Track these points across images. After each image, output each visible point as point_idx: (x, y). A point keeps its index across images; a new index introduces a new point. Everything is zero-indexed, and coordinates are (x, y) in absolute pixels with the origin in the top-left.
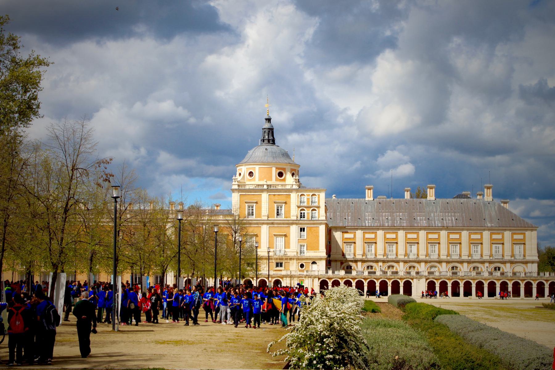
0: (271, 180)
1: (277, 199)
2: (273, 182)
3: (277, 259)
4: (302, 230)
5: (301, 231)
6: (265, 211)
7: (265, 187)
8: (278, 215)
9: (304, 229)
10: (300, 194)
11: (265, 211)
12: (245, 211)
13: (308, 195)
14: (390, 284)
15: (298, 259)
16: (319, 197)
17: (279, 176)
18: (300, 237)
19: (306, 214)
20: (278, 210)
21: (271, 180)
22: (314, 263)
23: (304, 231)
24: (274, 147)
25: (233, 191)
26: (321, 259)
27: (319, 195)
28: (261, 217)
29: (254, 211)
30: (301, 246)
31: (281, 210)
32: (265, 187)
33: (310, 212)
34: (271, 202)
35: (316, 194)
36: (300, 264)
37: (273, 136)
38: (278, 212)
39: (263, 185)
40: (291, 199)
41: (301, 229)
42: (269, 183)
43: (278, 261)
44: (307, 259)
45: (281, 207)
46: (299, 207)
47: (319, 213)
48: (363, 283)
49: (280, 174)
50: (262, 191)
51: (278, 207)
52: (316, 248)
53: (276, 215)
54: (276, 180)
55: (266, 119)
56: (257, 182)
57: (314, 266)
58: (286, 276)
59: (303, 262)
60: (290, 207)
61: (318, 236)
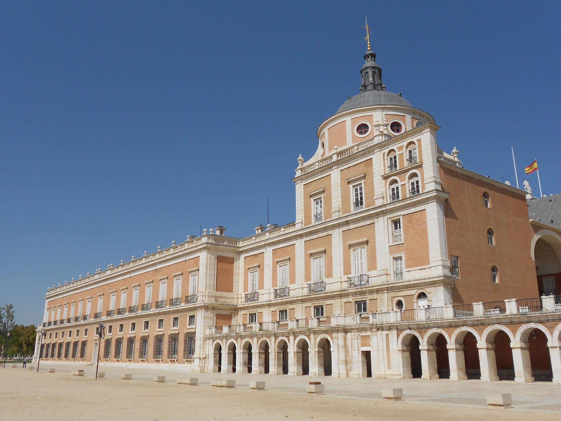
1: (352, 174)
3: (355, 294)
4: (396, 223)
7: (335, 158)
10: (387, 151)
11: (336, 202)
13: (400, 148)
15: (390, 289)
16: (420, 146)
22: (422, 295)
26: (433, 284)
30: (396, 259)
35: (414, 140)
36: (396, 300)
40: (374, 167)
43: (359, 298)
44: (407, 287)
46: (385, 178)
48: (509, 341)
57: (423, 303)
58: (337, 330)
60: (372, 183)
61: (425, 232)
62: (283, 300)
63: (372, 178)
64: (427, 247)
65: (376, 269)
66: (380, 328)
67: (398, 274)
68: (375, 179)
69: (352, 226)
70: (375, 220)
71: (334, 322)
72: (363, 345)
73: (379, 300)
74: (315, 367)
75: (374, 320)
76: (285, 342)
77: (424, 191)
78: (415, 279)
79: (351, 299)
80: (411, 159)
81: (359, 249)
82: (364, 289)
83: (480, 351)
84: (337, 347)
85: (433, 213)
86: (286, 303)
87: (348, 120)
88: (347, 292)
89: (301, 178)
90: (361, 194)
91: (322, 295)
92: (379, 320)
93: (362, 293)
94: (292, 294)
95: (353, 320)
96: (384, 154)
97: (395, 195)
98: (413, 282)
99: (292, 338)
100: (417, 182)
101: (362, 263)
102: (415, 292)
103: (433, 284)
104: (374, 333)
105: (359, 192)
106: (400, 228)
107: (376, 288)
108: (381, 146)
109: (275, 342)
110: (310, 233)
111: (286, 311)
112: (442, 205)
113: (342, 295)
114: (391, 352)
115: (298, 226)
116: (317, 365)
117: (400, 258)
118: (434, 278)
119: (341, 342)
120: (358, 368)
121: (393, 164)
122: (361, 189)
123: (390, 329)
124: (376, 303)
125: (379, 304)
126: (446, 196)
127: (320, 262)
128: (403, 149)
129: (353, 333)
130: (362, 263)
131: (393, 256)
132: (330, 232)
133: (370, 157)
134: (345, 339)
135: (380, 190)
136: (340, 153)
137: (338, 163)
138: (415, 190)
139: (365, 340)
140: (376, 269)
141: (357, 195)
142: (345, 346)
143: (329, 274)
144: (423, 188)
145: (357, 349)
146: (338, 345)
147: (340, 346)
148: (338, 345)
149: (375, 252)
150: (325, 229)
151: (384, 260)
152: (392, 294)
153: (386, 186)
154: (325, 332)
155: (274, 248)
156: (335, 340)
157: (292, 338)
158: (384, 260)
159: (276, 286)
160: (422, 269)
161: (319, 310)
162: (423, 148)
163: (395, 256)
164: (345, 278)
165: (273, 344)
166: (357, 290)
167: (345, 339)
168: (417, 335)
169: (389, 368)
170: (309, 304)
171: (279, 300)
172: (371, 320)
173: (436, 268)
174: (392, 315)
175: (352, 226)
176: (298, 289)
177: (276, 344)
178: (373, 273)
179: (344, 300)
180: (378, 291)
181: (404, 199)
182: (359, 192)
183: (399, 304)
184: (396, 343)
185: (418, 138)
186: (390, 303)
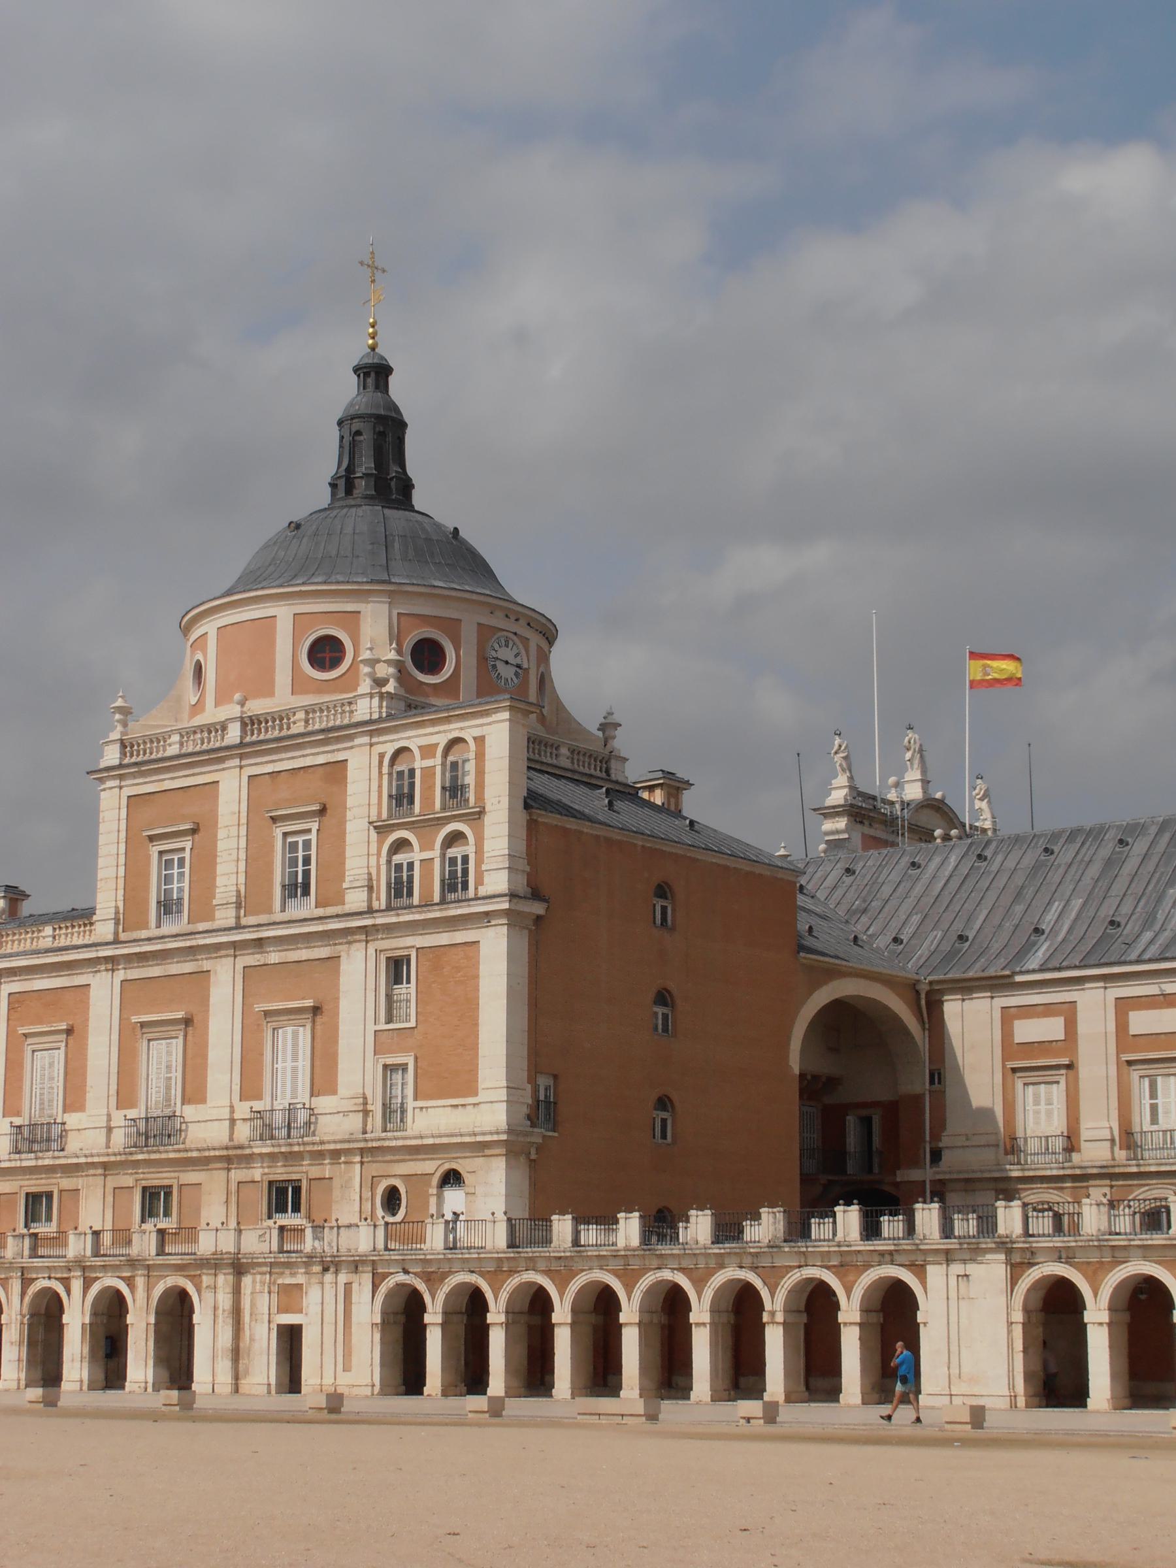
0: (271, 693)
2: (282, 697)
4: (397, 968)
6: (229, 877)
7: (234, 734)
10: (390, 749)
11: (229, 877)
12: (147, 889)
14: (775, 1304)
16: (480, 756)
17: (335, 662)
18: (389, 1020)
21: (271, 693)
22: (452, 1178)
25: (102, 774)
26: (480, 1148)
27: (480, 740)
32: (234, 734)
33: (436, 853)
34: (263, 815)
35: (468, 735)
40: (351, 789)
42: (257, 707)
43: (280, 1173)
46: (382, 830)
47: (479, 851)
49: (326, 652)
50: (216, 756)
52: (457, 1082)
54: (299, 684)
56: (212, 714)
58: (213, 1263)
59: (398, 1172)
62: (40, 1163)
63: (342, 823)
64: (475, 1047)
65: (333, 1091)
66: (330, 1265)
67: (393, 1113)
68: (350, 827)
69: (274, 957)
70: (342, 949)
71: (206, 1245)
72: (280, 1311)
73: (336, 1183)
74: (140, 1364)
75: (317, 1243)
76: (57, 1295)
77: (482, 891)
78: (435, 1132)
79: (257, 1173)
80: (454, 790)
81: (290, 1029)
82: (296, 1149)
83: (557, 1331)
84: (211, 1312)
85: (494, 953)
86: (51, 1170)
87: (283, 614)
88: (248, 1151)
89: (119, 771)
90: (307, 861)
91: (172, 1155)
92: (329, 1243)
93: (291, 1157)
94: (74, 1144)
95: (259, 1241)
96: (382, 756)
98: (430, 1141)
99: (77, 1285)
100: (465, 859)
101: (295, 1070)
102: (433, 1167)
103: (480, 1148)
104: (314, 1280)
105: (300, 854)
106: (408, 982)
107: (332, 1147)
108: (373, 728)
109: (23, 1294)
110: (143, 957)
111: (49, 1195)
112: (526, 932)
113: (232, 1157)
114: (353, 1330)
115: (104, 930)
116: (151, 1362)
117: (404, 1068)
118: (484, 1134)
119: (224, 1300)
120: (263, 1368)
121: (402, 798)
122: (307, 844)
123: (356, 1266)
124: (330, 1189)
125: (336, 1193)
126: (538, 909)
127: (169, 1053)
128: (434, 756)
129: (258, 1277)
130: (295, 1070)
131: (382, 1061)
132: (206, 965)
133: (340, 757)
134: (237, 1291)
135: (362, 856)
136: (249, 723)
137: (242, 750)
138: (455, 882)
139: (290, 1297)
140: (333, 1091)
141: (293, 862)
142: (236, 1312)
143: (194, 1092)
144: (479, 882)
145: (266, 1318)
146: (215, 1308)
147: (220, 1311)
148: (215, 1308)
149: (337, 1042)
150: (192, 951)
151: (357, 1070)
152: (374, 1169)
153: (379, 854)
154: (179, 1268)
155: (16, 986)
156: (208, 1296)
157: (77, 1285)
158: (357, 1070)
159: (18, 1114)
160: (457, 1106)
161: (154, 1200)
163: (389, 1061)
164: (243, 1109)
165: (16, 1299)
166: (276, 1150)
167: (237, 1291)
168: (421, 1286)
169: (347, 1368)
170: (126, 1180)
171: (28, 1161)
172: (309, 1243)
173: (490, 1109)
174: (365, 1232)
175: (274, 957)
176: (91, 1130)
177: (27, 1299)
178: (324, 1103)
179: (237, 1175)
180: (336, 1154)
181: (426, 905)
182: (300, 854)
183: (392, 1199)
184: (368, 1310)
185: (477, 732)
186: (367, 1194)
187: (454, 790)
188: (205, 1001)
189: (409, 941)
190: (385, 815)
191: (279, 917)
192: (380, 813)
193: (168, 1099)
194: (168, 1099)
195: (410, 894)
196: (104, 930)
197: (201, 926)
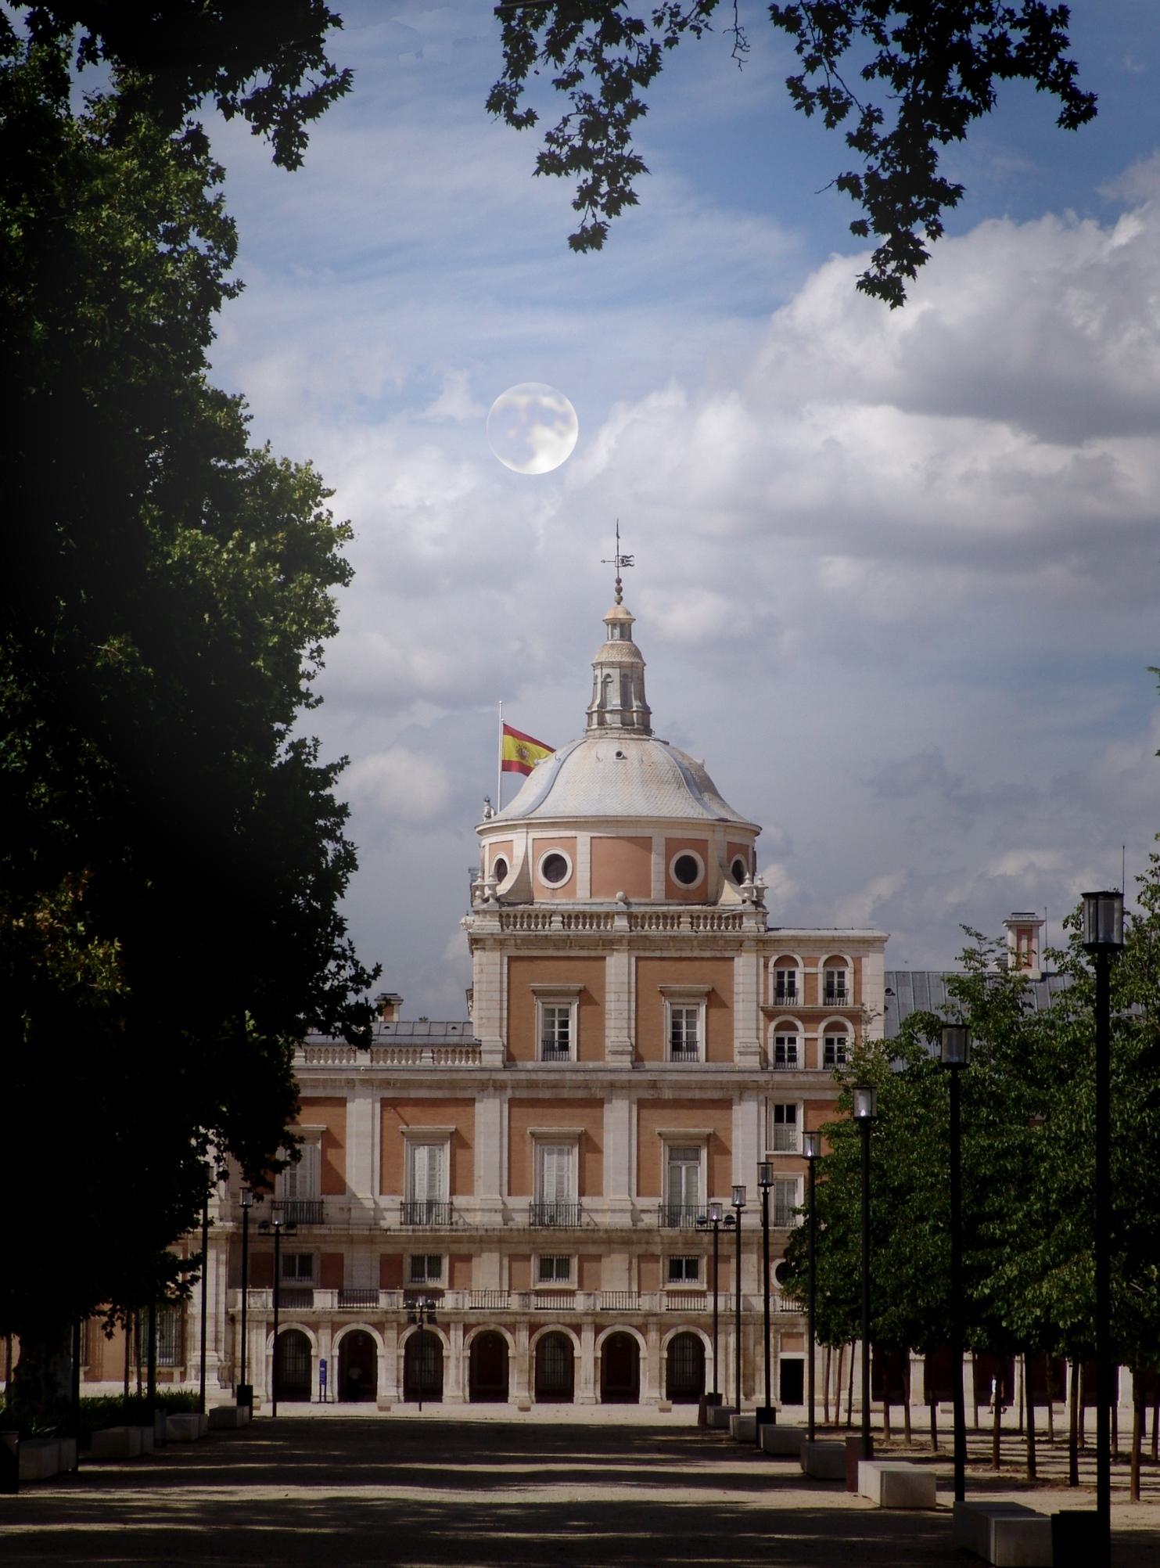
5: (779, 1119)
6: (617, 1030)
8: (676, 1047)
9: (792, 1110)
11: (617, 1030)
19: (800, 1045)
20: (676, 1026)
23: (792, 1119)
24: (651, 746)
28: (600, 1056)
29: (572, 1030)
31: (691, 1025)
37: (641, 697)
38: (676, 1036)
39: (609, 916)
41: (779, 1110)
45: (692, 1014)
46: (770, 1015)
51: (676, 1014)
53: (669, 1047)
55: (613, 623)
80: (834, 991)
97: (784, 1052)
128: (816, 966)
162: (864, 980)
187: (834, 991)
188: (599, 1123)
189: (797, 1094)
190: (771, 1001)
191: (670, 1065)
192: (766, 1001)
193: (560, 1192)
194: (560, 1192)
195: (793, 1059)
196: (495, 1060)
197: (591, 1065)
